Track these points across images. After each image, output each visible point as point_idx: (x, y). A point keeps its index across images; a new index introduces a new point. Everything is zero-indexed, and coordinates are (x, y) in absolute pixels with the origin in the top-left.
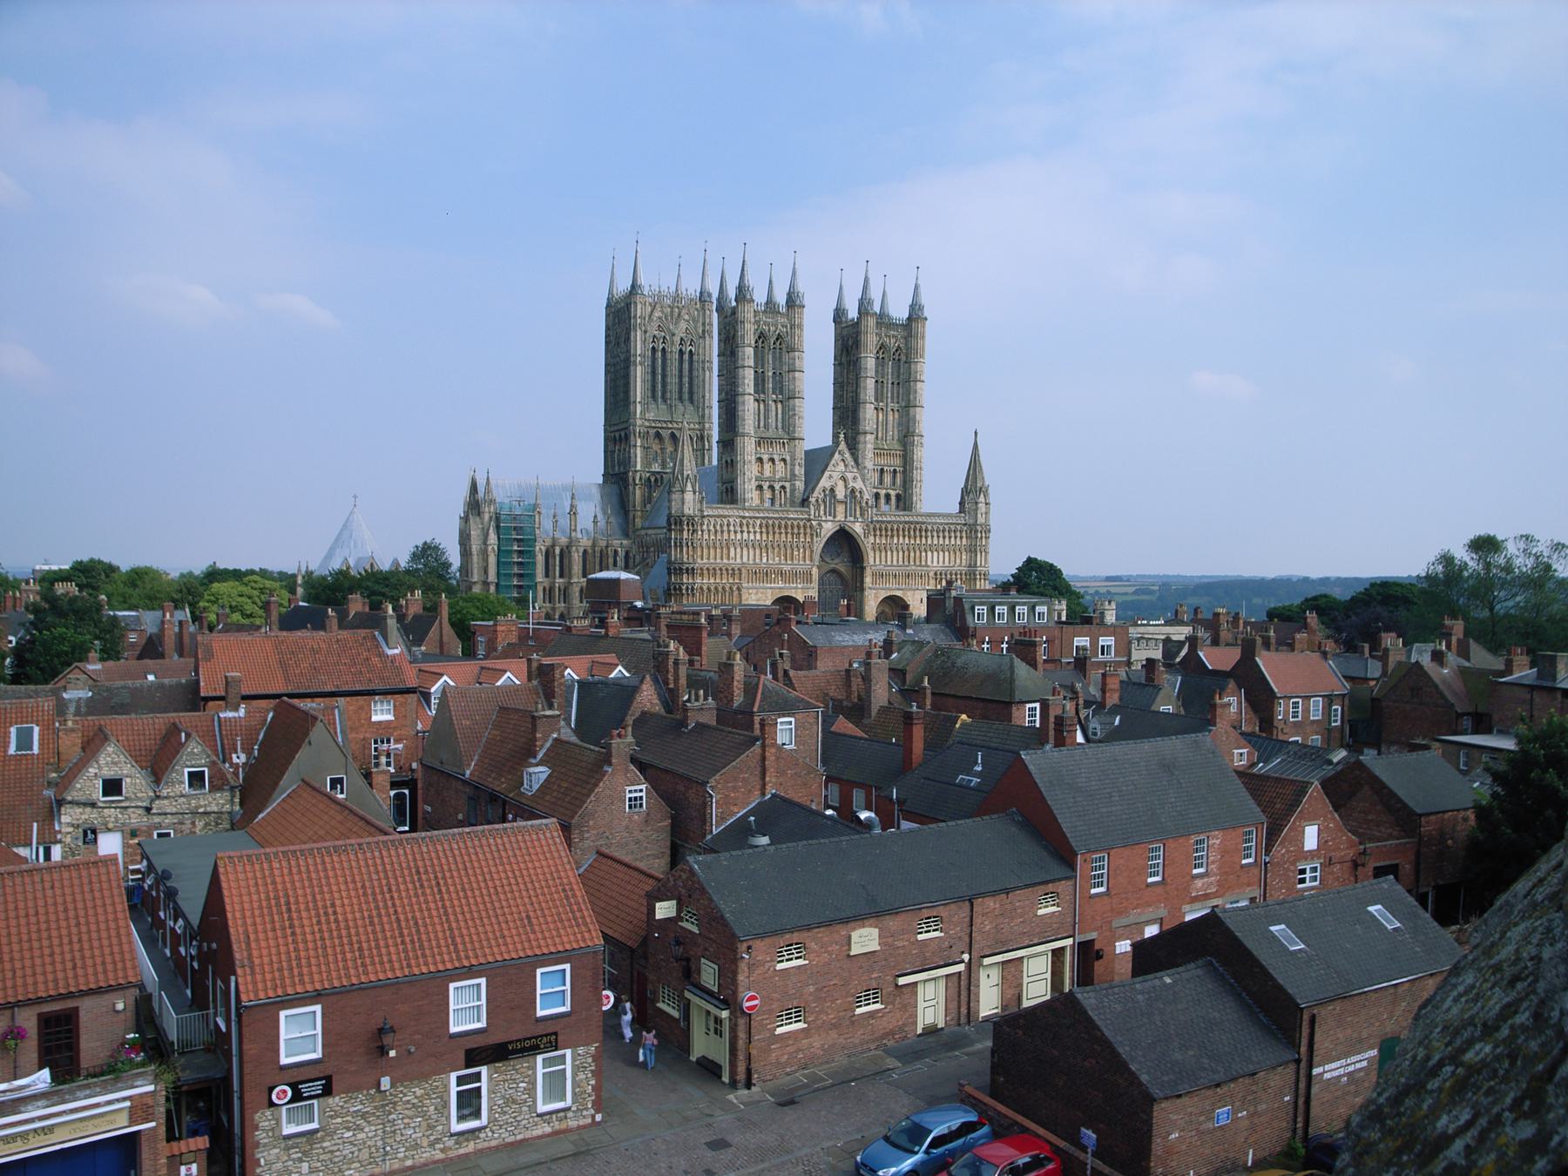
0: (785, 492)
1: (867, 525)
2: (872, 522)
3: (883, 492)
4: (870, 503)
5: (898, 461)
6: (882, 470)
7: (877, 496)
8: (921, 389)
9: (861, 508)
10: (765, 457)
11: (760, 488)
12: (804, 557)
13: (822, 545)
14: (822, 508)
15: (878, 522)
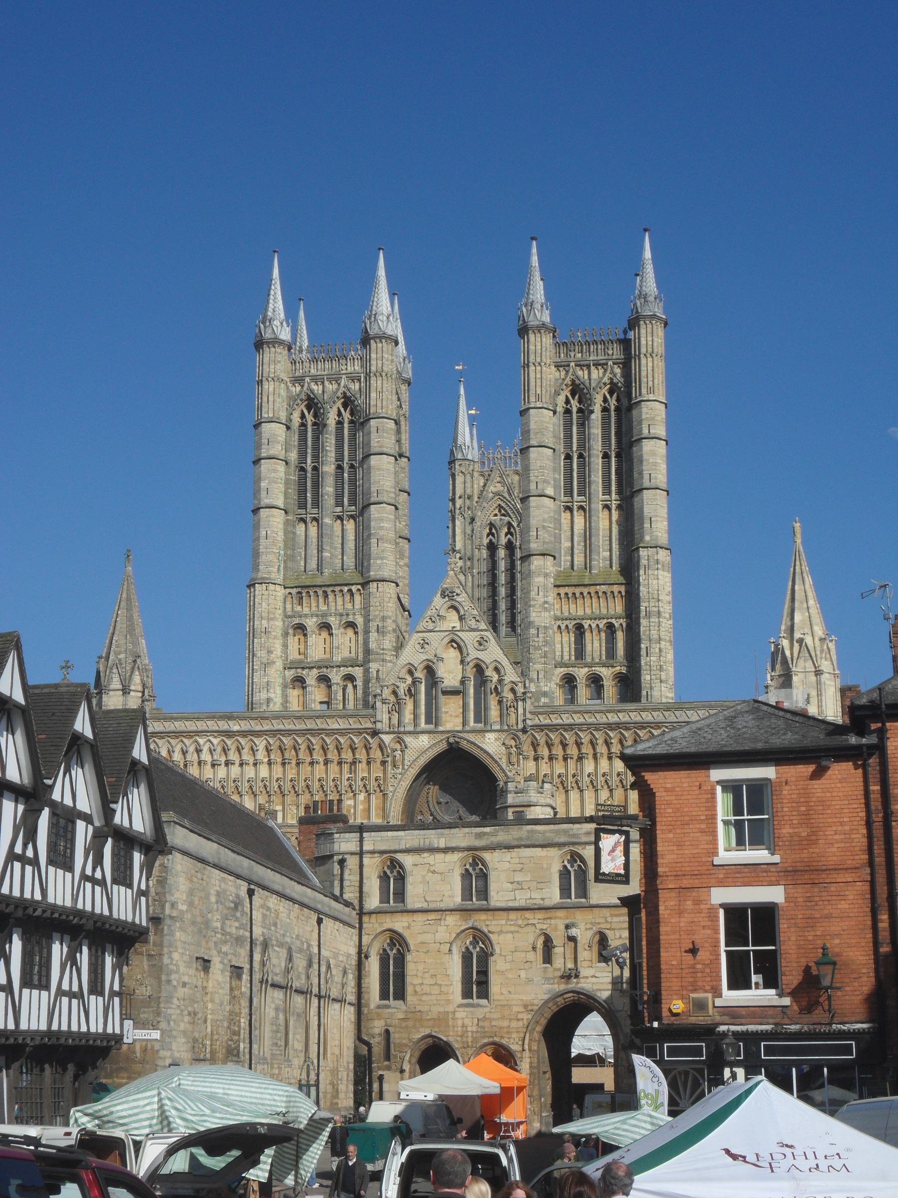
0: (355, 687)
1: (515, 738)
2: (524, 731)
3: (581, 673)
4: (520, 689)
5: (618, 607)
6: (579, 628)
7: (569, 681)
8: (653, 453)
9: (500, 702)
10: (311, 623)
11: (300, 681)
12: (368, 810)
13: (406, 783)
14: (409, 707)
15: (541, 728)
